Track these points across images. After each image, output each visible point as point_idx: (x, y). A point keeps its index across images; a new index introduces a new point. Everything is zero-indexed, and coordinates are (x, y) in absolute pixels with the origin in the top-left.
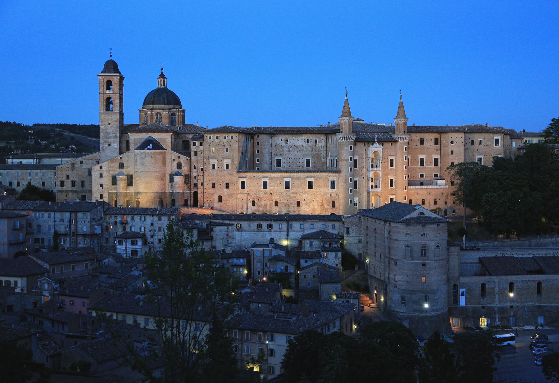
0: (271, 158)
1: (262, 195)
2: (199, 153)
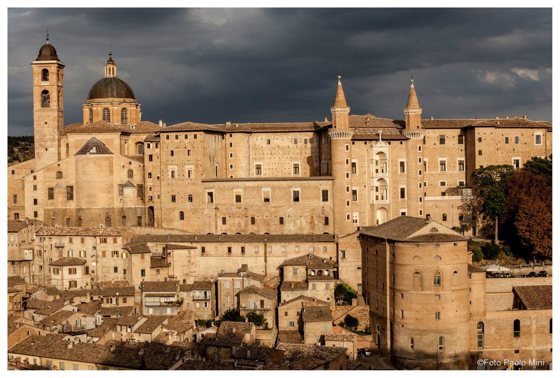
0: (249, 164)
1: (234, 210)
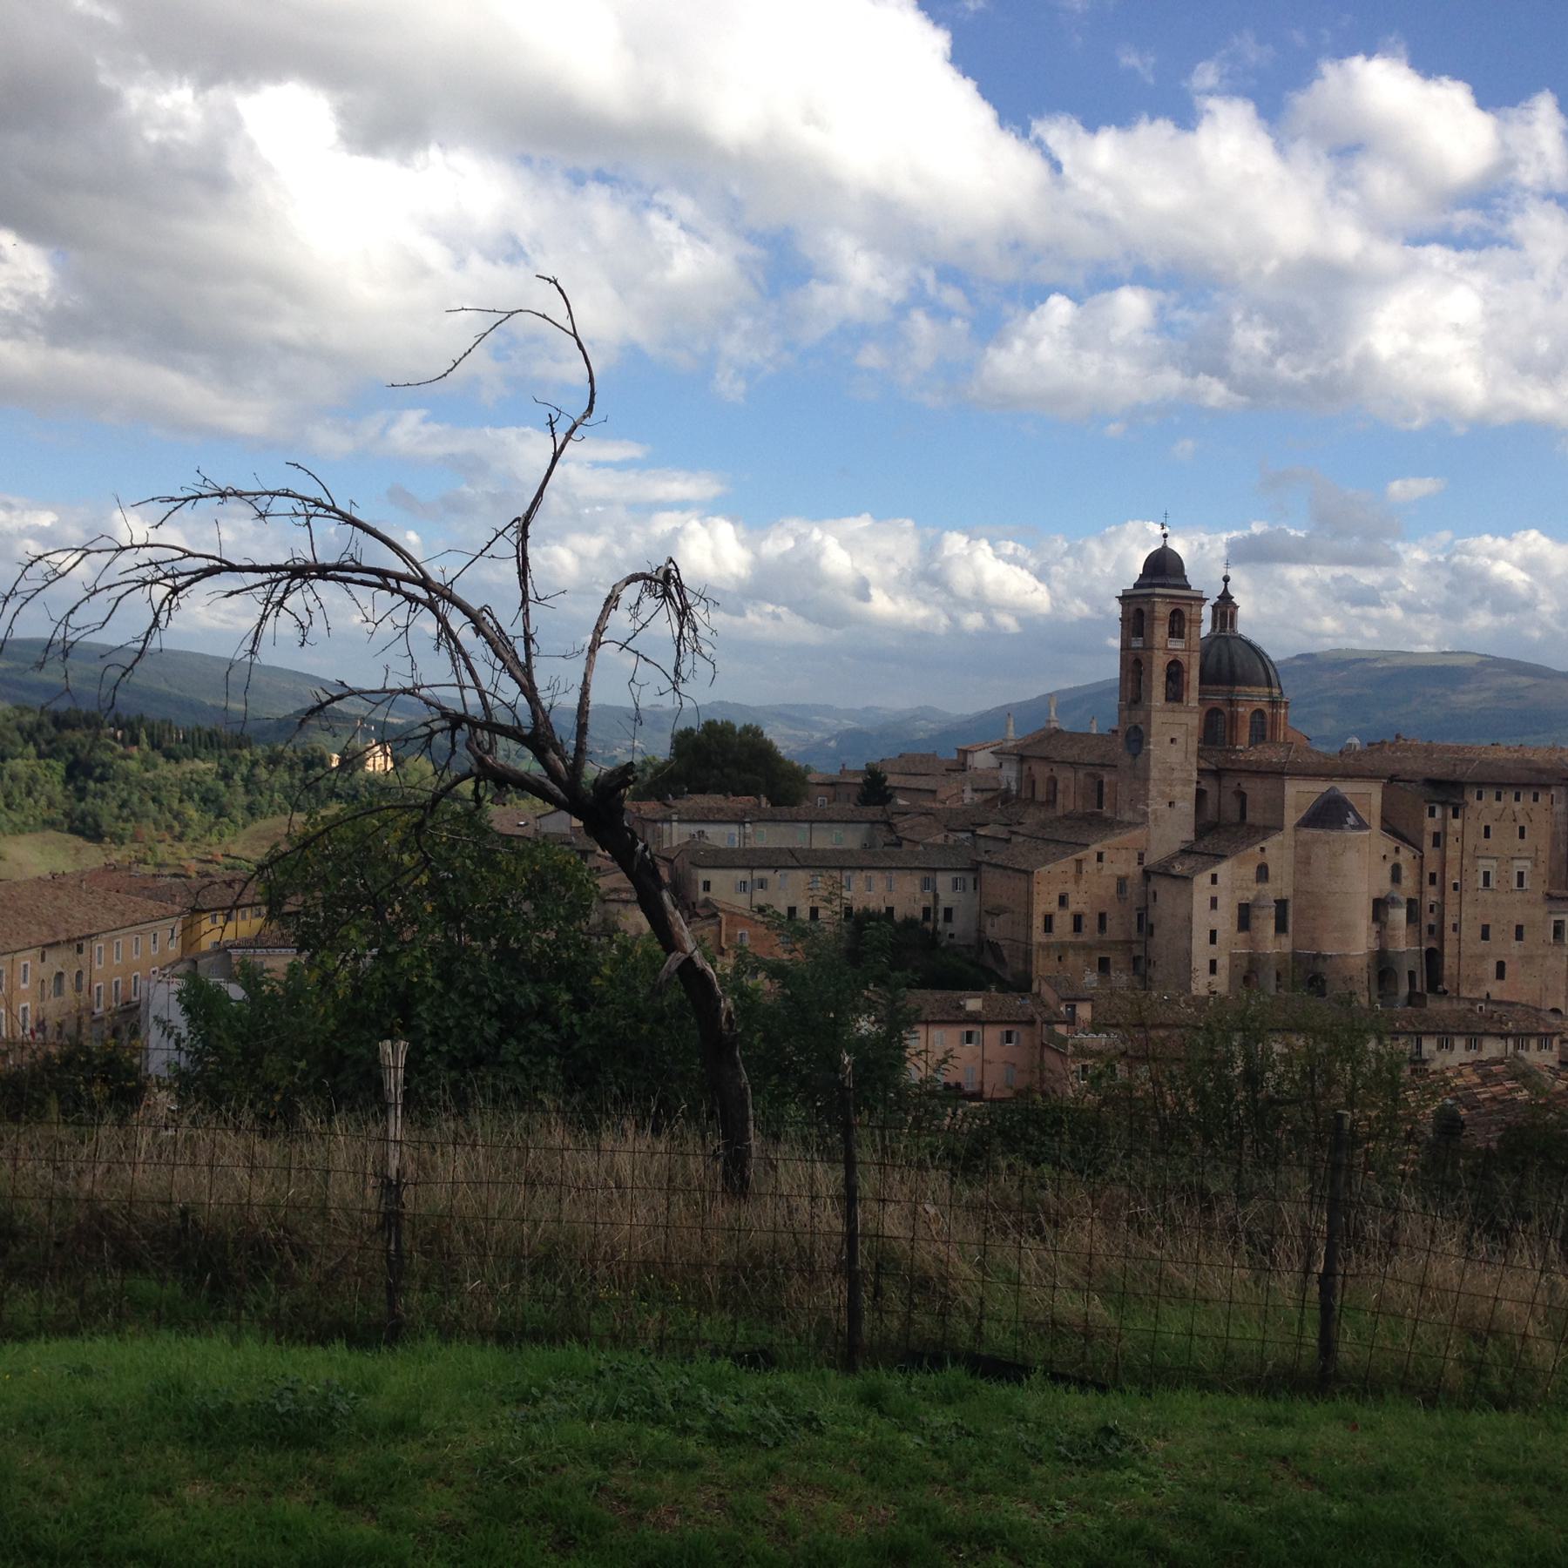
2: (1450, 840)
